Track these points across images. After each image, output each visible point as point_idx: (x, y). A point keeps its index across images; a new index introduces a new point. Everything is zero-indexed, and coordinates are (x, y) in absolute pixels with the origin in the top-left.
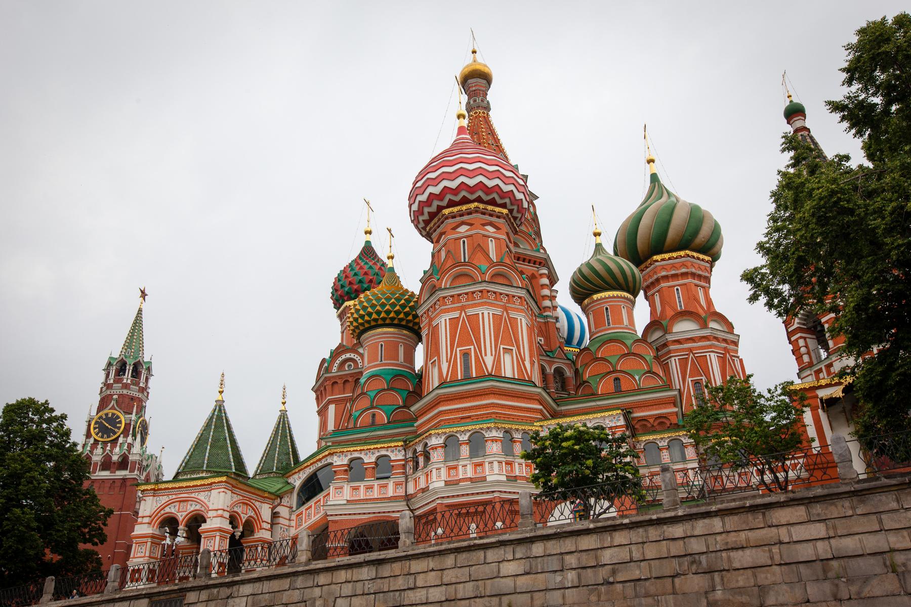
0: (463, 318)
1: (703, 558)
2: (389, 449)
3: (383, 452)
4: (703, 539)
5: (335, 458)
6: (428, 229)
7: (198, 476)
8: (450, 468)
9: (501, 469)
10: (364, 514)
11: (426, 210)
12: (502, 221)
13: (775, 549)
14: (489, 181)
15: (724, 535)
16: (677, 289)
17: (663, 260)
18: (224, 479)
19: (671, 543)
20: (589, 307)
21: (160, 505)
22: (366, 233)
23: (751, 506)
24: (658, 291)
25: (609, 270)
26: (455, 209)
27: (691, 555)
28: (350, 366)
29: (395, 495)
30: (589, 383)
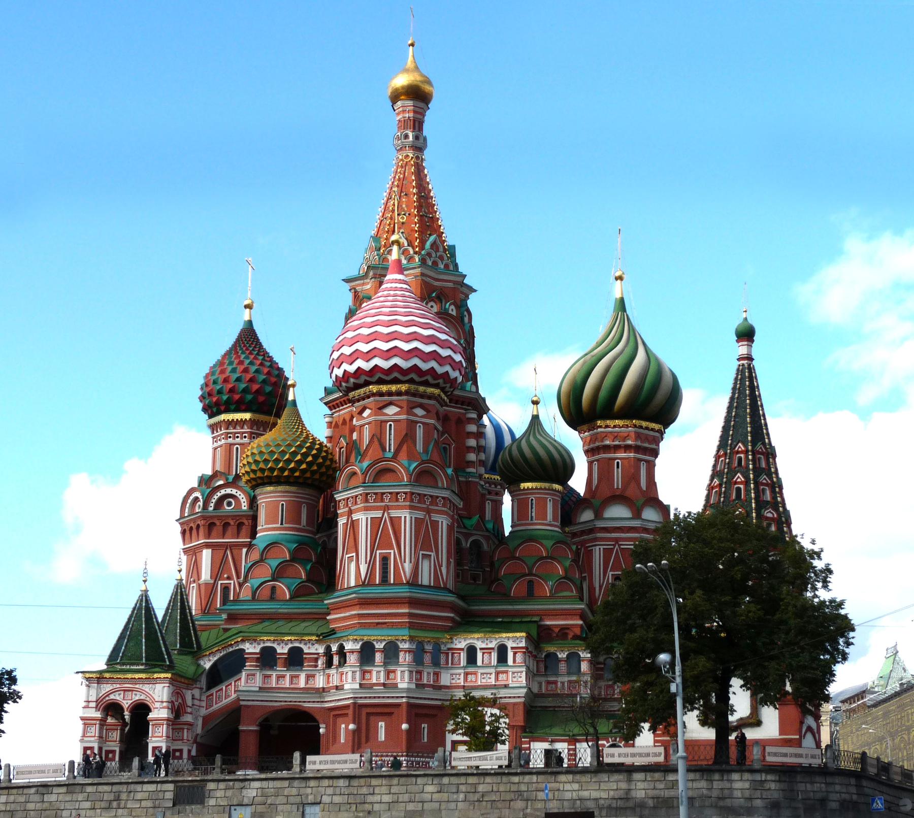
0: (385, 519)
1: (525, 794)
2: (302, 641)
7: (138, 667)
8: (364, 673)
9: (411, 678)
13: (556, 793)
14: (424, 363)
19: (512, 785)
21: (104, 692)
22: (246, 307)
26: (384, 388)
27: (520, 791)
29: (308, 686)
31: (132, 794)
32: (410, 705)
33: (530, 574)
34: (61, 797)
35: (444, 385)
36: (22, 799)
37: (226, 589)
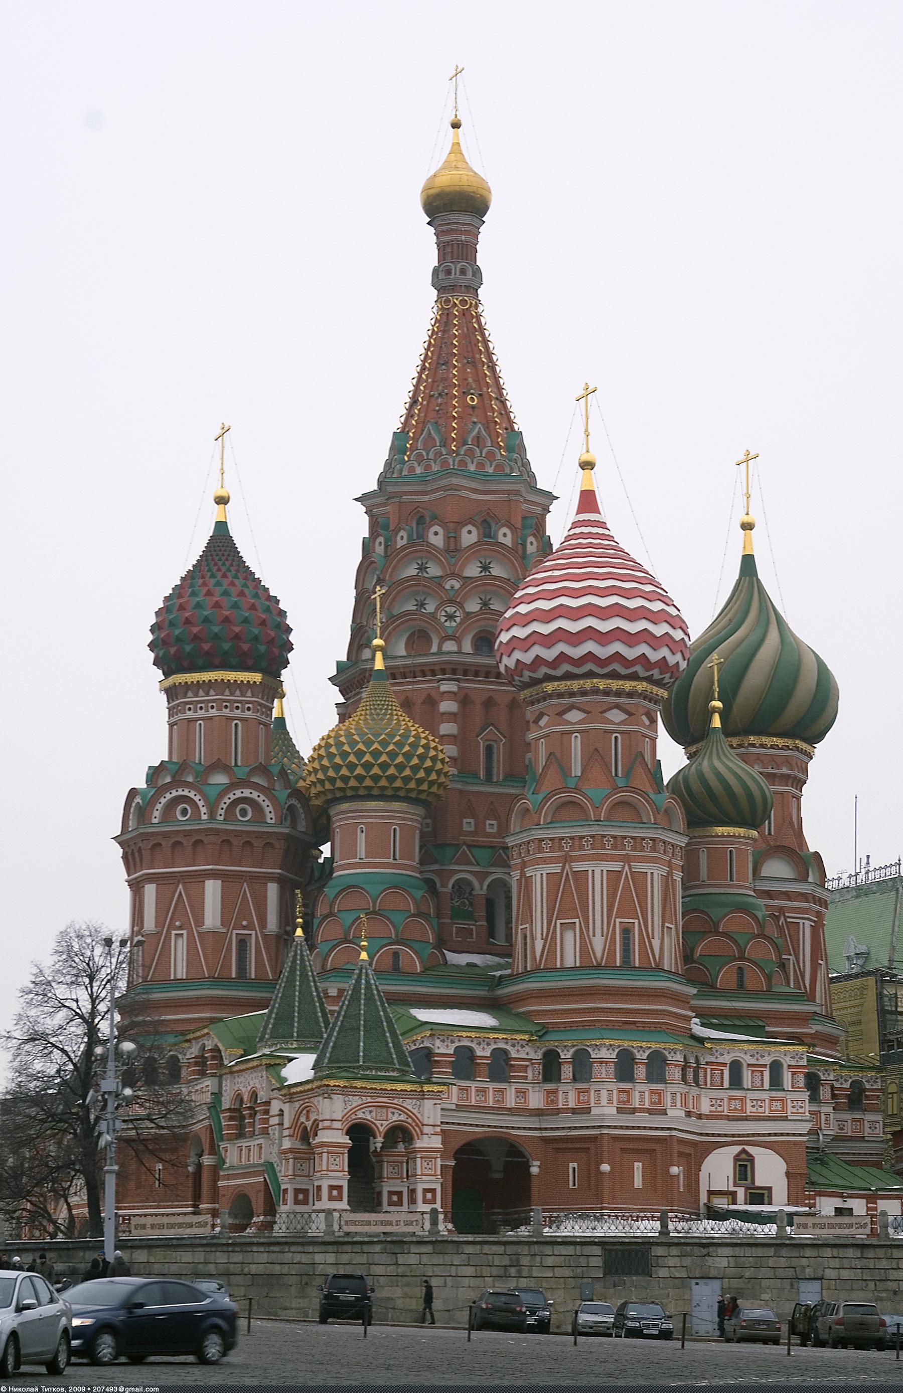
5: (438, 1043)
7: (387, 1074)
10: (477, 1126)
25: (750, 795)
26: (615, 685)
31: (538, 1258)
32: (681, 1141)
33: (742, 958)
34: (425, 1259)
36: (363, 1259)
37: (243, 943)
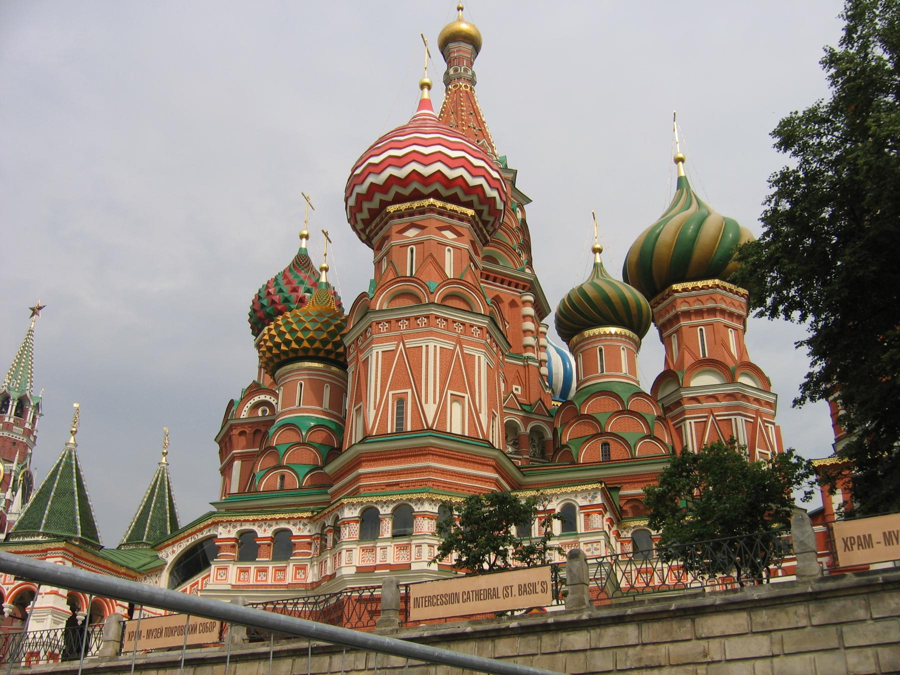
3: (283, 525)
4: (611, 652)
5: (220, 529)
6: (367, 231)
7: (33, 539)
11: (366, 205)
12: (466, 224)
15: (638, 648)
16: (701, 330)
17: (685, 290)
18: (62, 545)
20: (576, 348)
23: (678, 610)
24: (677, 332)
26: (404, 206)
28: (264, 411)
29: (295, 581)
30: (569, 448)
35: (480, 208)
